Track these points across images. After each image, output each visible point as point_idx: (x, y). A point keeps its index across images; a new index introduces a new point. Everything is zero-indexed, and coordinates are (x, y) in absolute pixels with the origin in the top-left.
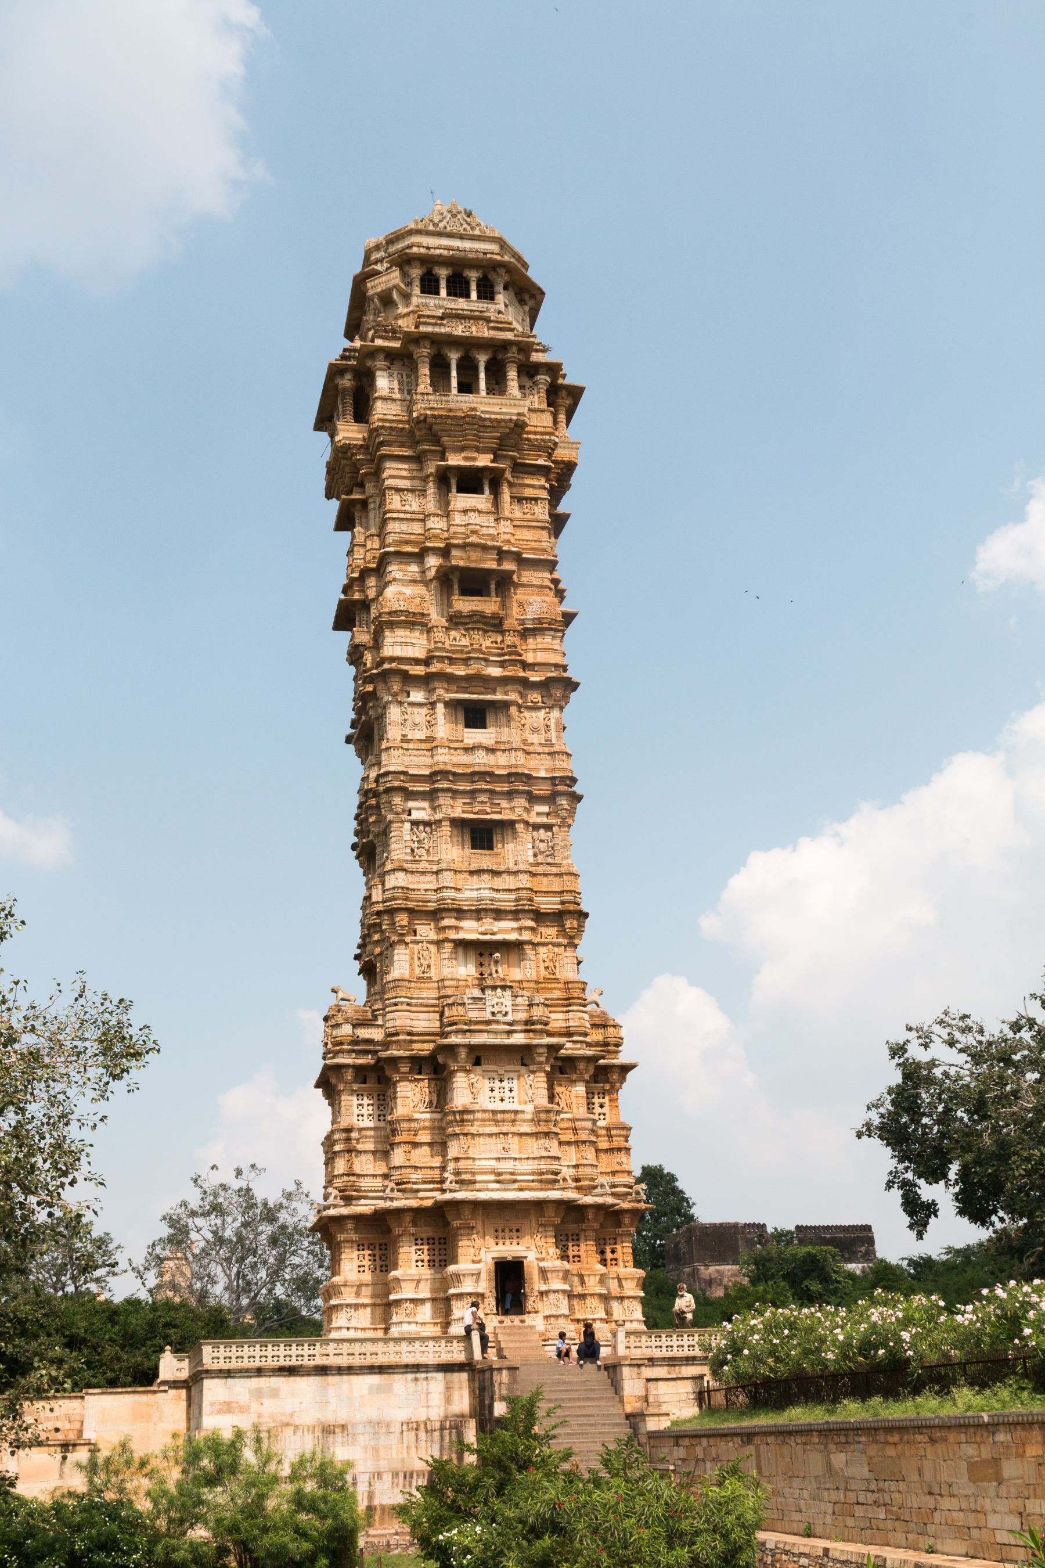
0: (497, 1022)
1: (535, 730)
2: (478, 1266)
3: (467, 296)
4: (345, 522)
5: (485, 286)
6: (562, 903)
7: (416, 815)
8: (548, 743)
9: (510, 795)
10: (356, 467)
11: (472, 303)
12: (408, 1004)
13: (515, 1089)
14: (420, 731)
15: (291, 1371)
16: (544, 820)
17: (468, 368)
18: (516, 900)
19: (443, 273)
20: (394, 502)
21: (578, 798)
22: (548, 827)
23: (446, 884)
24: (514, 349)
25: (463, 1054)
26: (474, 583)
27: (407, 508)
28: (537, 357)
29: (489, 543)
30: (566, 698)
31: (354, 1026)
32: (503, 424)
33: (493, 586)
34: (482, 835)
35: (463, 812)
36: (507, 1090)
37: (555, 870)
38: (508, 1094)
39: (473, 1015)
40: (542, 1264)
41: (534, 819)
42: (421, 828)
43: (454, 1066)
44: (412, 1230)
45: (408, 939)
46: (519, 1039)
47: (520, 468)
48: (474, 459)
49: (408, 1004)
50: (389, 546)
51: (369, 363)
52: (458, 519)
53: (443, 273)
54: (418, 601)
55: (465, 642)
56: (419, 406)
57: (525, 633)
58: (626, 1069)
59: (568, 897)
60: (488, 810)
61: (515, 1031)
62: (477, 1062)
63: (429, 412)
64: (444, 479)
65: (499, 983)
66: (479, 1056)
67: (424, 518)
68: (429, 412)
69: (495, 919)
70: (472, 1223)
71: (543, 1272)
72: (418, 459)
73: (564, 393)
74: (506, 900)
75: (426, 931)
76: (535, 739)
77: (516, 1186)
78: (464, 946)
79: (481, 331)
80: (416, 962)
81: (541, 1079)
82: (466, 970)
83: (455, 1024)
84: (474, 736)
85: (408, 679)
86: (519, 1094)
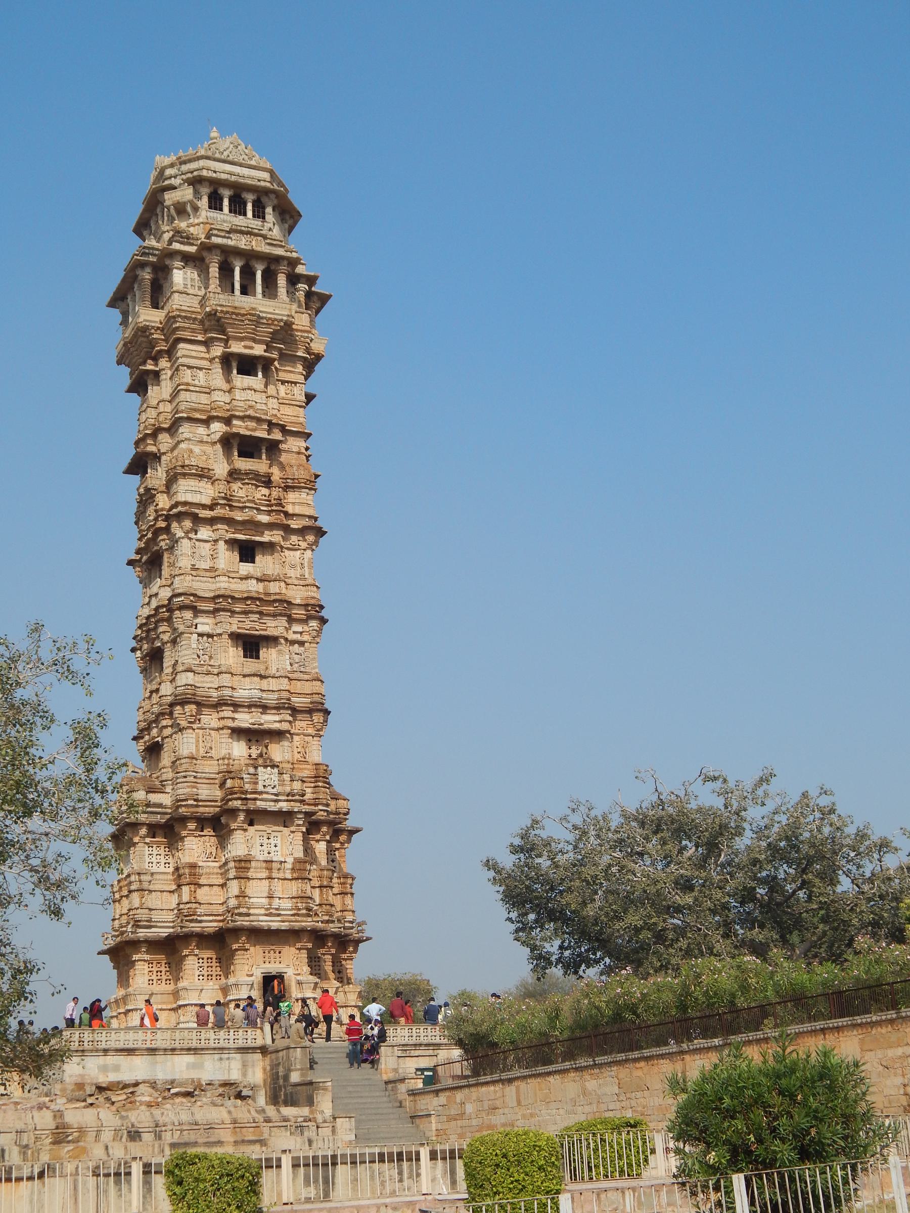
0: (267, 793)
1: (293, 566)
2: (251, 978)
3: (245, 214)
4: (139, 385)
5: (258, 207)
6: (311, 703)
7: (201, 629)
8: (302, 577)
9: (274, 616)
10: (152, 344)
11: (248, 220)
12: (195, 777)
13: (279, 843)
14: (202, 560)
15: (130, 1051)
16: (297, 637)
17: (248, 274)
18: (278, 699)
19: (226, 193)
20: (186, 376)
21: (323, 621)
22: (302, 643)
23: (225, 684)
24: (286, 263)
25: (242, 817)
26: (248, 447)
27: (196, 382)
28: (300, 269)
29: (263, 417)
30: (316, 543)
31: (148, 792)
32: (276, 323)
33: (264, 451)
35: (238, 628)
36: (272, 845)
37: (306, 677)
38: (273, 849)
39: (248, 787)
40: (299, 978)
41: (291, 636)
42: (205, 638)
43: (233, 826)
44: (197, 952)
45: (195, 726)
46: (284, 806)
47: (283, 357)
48: (251, 348)
49: (195, 777)
50: (182, 412)
51: (167, 262)
52: (238, 395)
53: (226, 193)
54: (204, 458)
55: (241, 493)
56: (212, 302)
57: (287, 488)
58: (352, 832)
59: (316, 698)
60: (257, 628)
61: (280, 801)
62: (251, 824)
63: (219, 308)
64: (226, 360)
65: (268, 763)
66: (254, 817)
67: (209, 391)
68: (219, 308)
69: (262, 713)
70: (247, 946)
71: (299, 983)
72: (207, 343)
73: (315, 298)
74: (271, 699)
75: (210, 719)
76: (292, 573)
77: (279, 918)
78: (238, 733)
79: (260, 246)
80: (201, 743)
81: (299, 836)
82: (239, 750)
83: (236, 793)
84: (246, 568)
85: (197, 520)
86: (282, 849)
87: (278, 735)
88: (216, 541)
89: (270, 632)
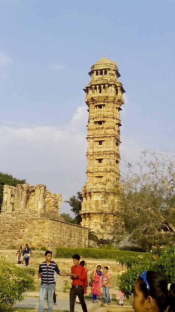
17: (100, 88)
19: (99, 72)
22: (110, 159)
26: (100, 123)
34: (100, 161)
88: (94, 141)
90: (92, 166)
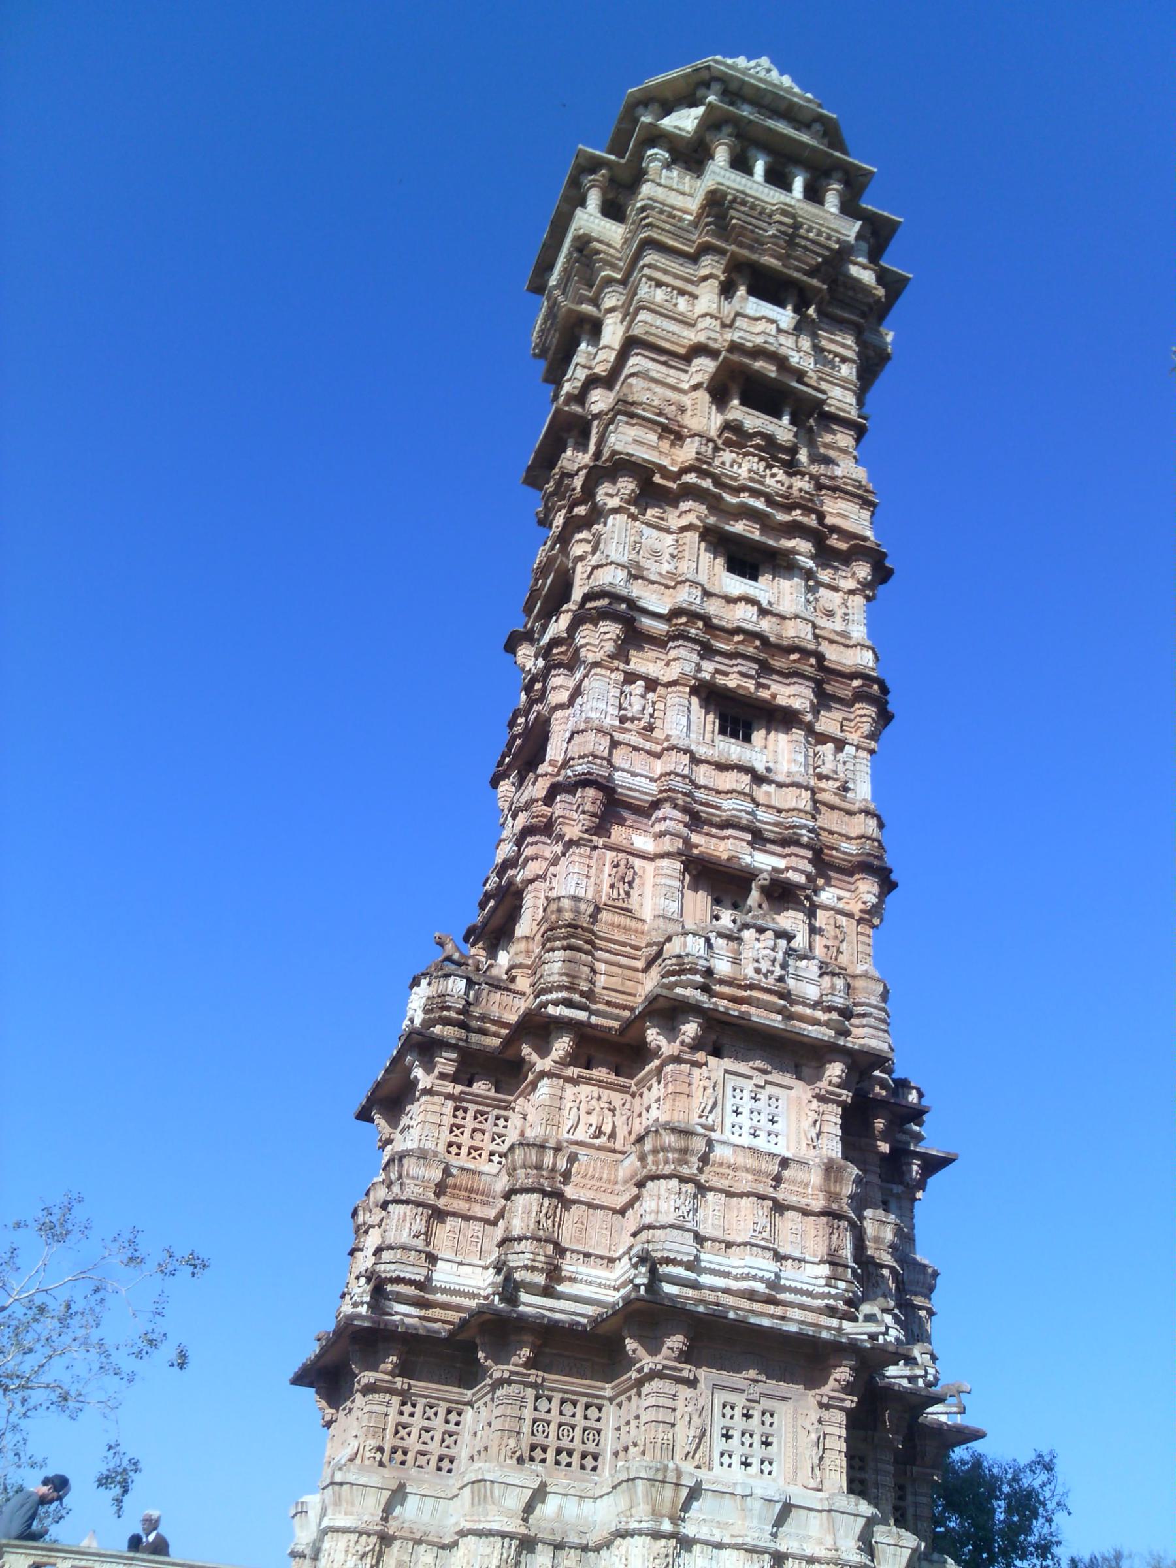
62: (717, 1053)
87: (781, 894)
89: (781, 701)
90: (636, 740)
